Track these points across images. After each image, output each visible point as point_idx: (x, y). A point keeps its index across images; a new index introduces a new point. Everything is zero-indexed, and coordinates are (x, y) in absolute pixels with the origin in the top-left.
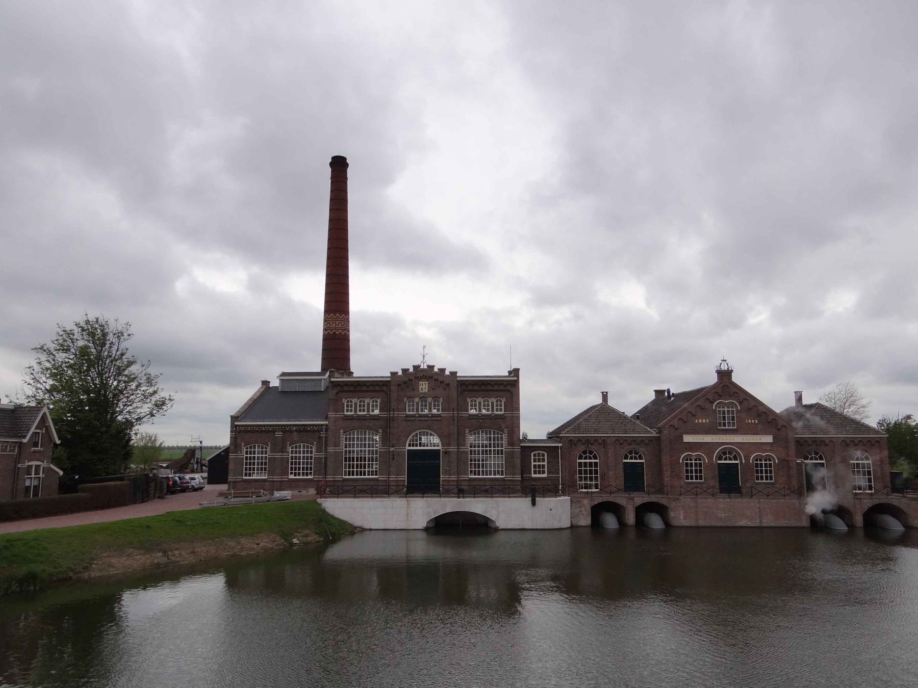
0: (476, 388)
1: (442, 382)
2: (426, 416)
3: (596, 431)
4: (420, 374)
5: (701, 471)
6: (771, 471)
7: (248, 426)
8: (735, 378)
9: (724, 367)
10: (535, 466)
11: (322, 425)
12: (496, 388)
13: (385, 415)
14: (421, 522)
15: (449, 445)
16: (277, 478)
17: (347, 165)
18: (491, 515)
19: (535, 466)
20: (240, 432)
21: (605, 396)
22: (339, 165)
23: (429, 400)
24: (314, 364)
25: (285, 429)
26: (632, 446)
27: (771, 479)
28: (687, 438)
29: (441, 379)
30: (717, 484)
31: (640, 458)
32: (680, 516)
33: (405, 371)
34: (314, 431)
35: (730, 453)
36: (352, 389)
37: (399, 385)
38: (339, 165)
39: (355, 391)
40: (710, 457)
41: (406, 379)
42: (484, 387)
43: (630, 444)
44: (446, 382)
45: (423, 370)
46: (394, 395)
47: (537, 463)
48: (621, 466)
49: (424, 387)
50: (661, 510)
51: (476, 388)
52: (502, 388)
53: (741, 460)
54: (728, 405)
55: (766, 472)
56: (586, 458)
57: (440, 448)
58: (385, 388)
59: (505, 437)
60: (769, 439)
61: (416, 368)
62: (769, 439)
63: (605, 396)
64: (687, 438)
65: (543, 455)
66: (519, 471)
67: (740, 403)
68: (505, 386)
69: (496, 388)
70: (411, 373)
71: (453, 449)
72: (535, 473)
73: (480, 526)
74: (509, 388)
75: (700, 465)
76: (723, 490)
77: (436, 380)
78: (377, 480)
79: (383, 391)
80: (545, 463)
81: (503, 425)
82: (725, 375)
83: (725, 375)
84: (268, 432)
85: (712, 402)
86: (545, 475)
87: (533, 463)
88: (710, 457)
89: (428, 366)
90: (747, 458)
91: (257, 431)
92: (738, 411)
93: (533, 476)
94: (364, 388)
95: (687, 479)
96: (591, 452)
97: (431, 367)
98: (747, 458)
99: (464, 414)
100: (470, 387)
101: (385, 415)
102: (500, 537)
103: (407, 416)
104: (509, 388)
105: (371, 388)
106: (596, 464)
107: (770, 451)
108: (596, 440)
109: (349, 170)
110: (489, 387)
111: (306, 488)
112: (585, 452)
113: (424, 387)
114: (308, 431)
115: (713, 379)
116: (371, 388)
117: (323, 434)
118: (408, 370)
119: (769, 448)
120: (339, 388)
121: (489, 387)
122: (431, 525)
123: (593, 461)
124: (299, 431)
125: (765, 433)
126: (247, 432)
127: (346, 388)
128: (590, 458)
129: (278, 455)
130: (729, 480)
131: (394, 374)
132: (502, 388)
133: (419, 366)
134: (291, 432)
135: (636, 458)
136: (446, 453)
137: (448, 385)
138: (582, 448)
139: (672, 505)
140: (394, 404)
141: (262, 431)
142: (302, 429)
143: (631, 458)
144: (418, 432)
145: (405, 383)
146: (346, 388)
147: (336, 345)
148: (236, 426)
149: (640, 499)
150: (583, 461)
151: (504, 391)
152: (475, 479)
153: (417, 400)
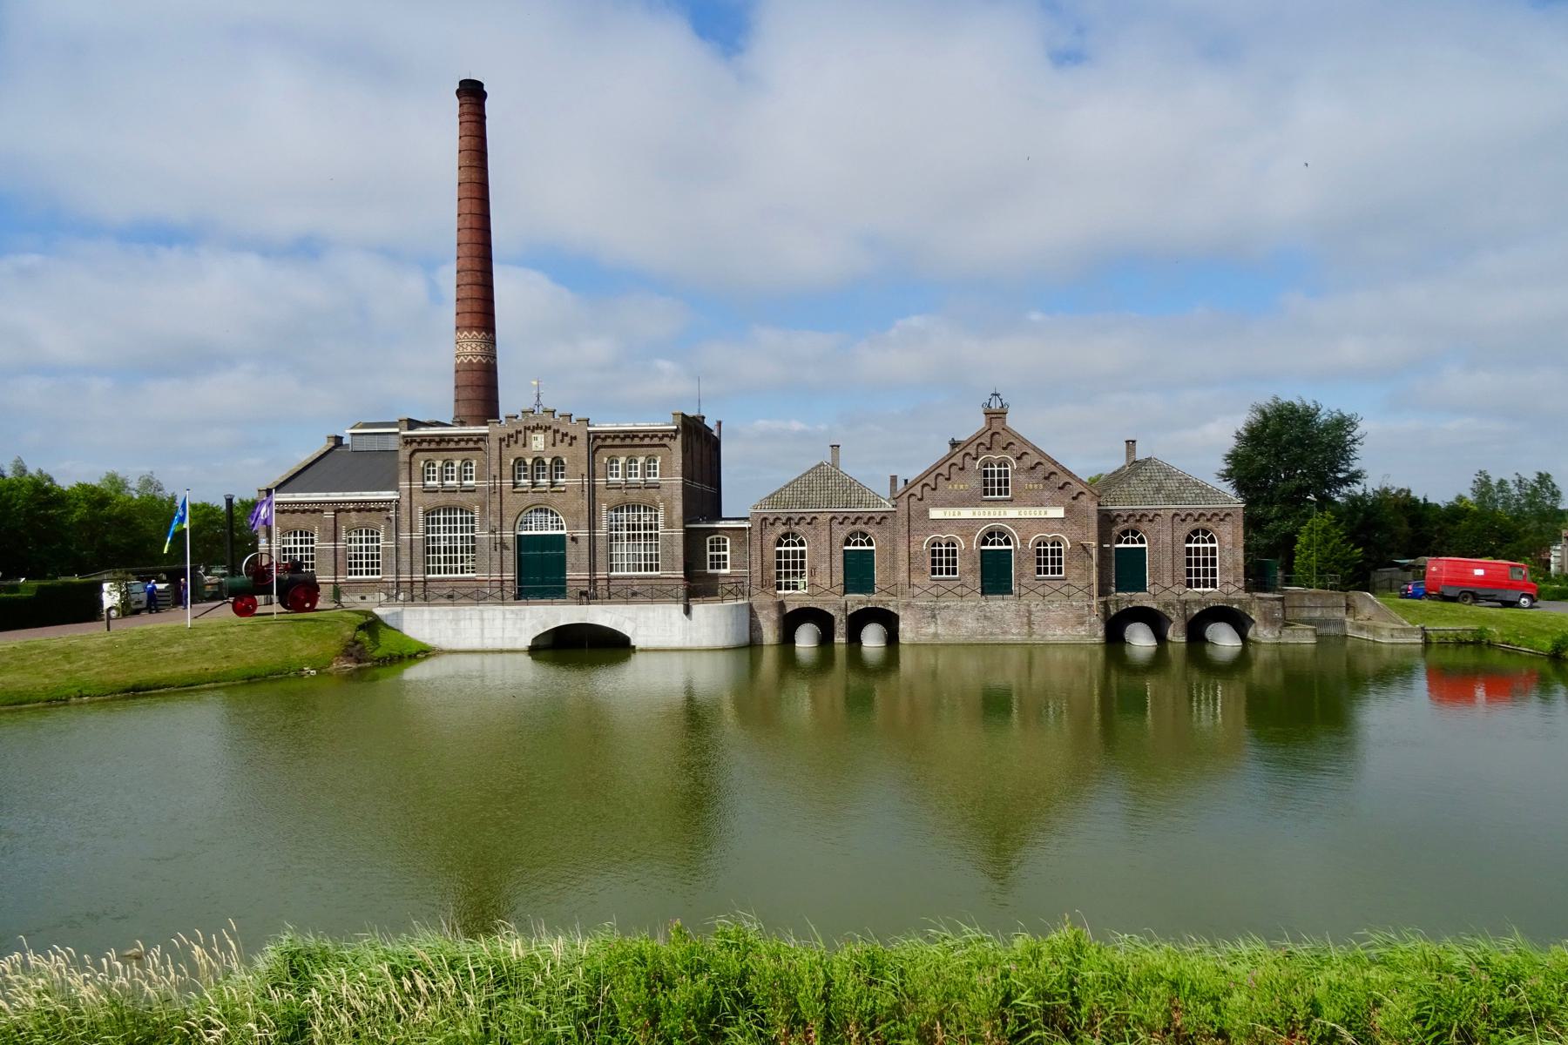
0: (618, 442)
3: (804, 505)
5: (954, 562)
8: (1012, 421)
9: (996, 405)
10: (712, 557)
14: (526, 642)
15: (578, 527)
17: (484, 95)
18: (626, 629)
19: (712, 557)
22: (472, 93)
25: (339, 509)
27: (1060, 572)
28: (935, 513)
30: (978, 583)
34: (380, 510)
36: (433, 446)
37: (501, 440)
38: (472, 93)
42: (628, 442)
49: (538, 442)
50: (889, 621)
56: (787, 545)
60: (1059, 513)
62: (1059, 513)
64: (935, 513)
66: (680, 564)
69: (647, 441)
72: (712, 567)
73: (612, 646)
74: (666, 441)
75: (954, 552)
76: (985, 591)
77: (556, 431)
80: (728, 553)
81: (658, 498)
82: (995, 416)
83: (995, 416)
84: (314, 511)
85: (976, 459)
86: (727, 571)
87: (709, 553)
93: (709, 571)
94: (452, 445)
95: (934, 572)
96: (794, 535)
98: (1024, 541)
100: (609, 442)
102: (637, 660)
104: (666, 441)
105: (462, 445)
106: (802, 554)
107: (1061, 531)
109: (487, 103)
110: (637, 441)
111: (372, 592)
112: (786, 536)
114: (370, 510)
115: (980, 422)
117: (392, 514)
120: (415, 446)
121: (637, 441)
122: (542, 643)
124: (359, 510)
125: (1055, 505)
130: (995, 574)
135: (862, 544)
139: (901, 614)
142: (363, 507)
145: (510, 436)
149: (857, 601)
152: (616, 578)
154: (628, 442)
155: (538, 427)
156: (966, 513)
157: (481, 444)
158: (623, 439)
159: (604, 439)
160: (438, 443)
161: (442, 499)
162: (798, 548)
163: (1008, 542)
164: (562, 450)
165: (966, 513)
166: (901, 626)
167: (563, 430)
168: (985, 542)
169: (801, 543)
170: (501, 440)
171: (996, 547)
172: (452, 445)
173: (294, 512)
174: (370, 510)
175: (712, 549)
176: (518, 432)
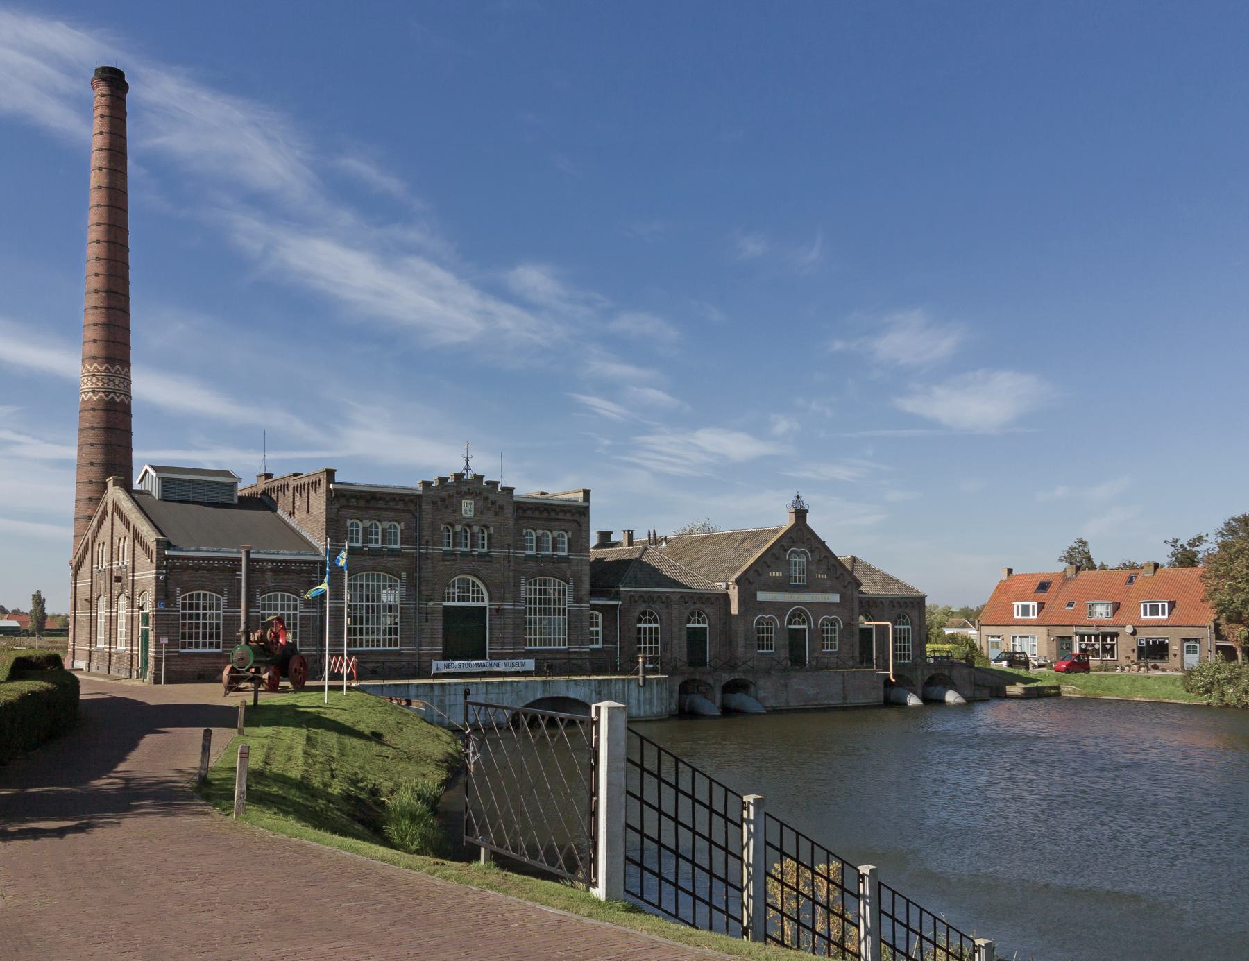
1: (493, 503)
2: (470, 554)
4: (464, 488)
7: (189, 558)
12: (561, 516)
13: (408, 549)
15: (503, 599)
20: (174, 567)
23: (476, 529)
28: (762, 596)
29: (492, 497)
33: (442, 480)
35: (800, 616)
39: (367, 508)
40: (782, 622)
41: (444, 494)
42: (545, 515)
44: (500, 502)
45: (467, 481)
46: (427, 519)
48: (685, 632)
49: (468, 507)
51: (536, 514)
52: (568, 516)
54: (798, 554)
56: (645, 622)
57: (486, 603)
58: (411, 507)
59: (569, 589)
60: (835, 598)
61: (458, 476)
62: (835, 598)
64: (762, 596)
65: (597, 617)
67: (812, 552)
70: (449, 486)
71: (508, 605)
77: (486, 499)
78: (398, 653)
80: (599, 629)
81: (569, 572)
86: (599, 646)
88: (782, 622)
90: (816, 624)
91: (204, 568)
96: (651, 614)
97: (479, 478)
98: (816, 624)
99: (521, 553)
101: (408, 549)
103: (445, 553)
104: (577, 517)
106: (656, 628)
108: (659, 595)
112: (644, 613)
113: (468, 507)
116: (392, 504)
118: (446, 479)
120: (343, 500)
123: (653, 625)
125: (834, 591)
126: (185, 568)
131: (426, 484)
133: (462, 475)
134: (263, 571)
136: (497, 611)
137: (501, 507)
138: (642, 607)
140: (427, 534)
141: (214, 569)
145: (443, 500)
148: (167, 558)
151: (570, 521)
153: (458, 528)
159: (524, 511)
160: (368, 501)
162: (653, 625)
163: (804, 623)
164: (489, 517)
168: (790, 622)
169: (655, 621)
171: (797, 627)
172: (381, 504)
173: (199, 569)
174: (287, 571)
176: (450, 496)
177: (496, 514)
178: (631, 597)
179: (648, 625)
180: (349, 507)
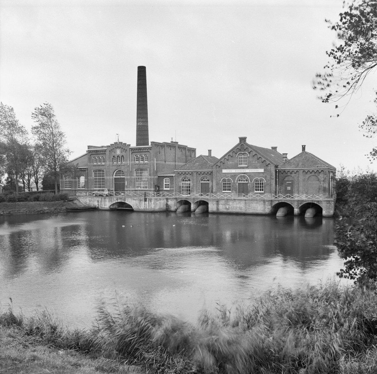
0: (137, 151)
6: (256, 187)
8: (248, 141)
11: (86, 168)
16: (73, 189)
19: (165, 184)
21: (210, 151)
24: (131, 140)
26: (204, 175)
28: (224, 171)
31: (208, 181)
32: (212, 207)
34: (84, 171)
40: (234, 180)
42: (139, 151)
43: (203, 174)
47: (166, 183)
51: (137, 151)
53: (249, 181)
54: (243, 154)
55: (260, 187)
56: (185, 181)
60: (262, 170)
62: (262, 170)
63: (210, 151)
64: (224, 171)
67: (249, 153)
68: (148, 150)
69: (144, 150)
72: (165, 187)
77: (122, 148)
79: (105, 154)
82: (243, 140)
83: (243, 140)
85: (236, 153)
87: (164, 183)
88: (234, 180)
89: (120, 143)
92: (248, 157)
93: (165, 189)
94: (99, 153)
97: (122, 143)
104: (149, 150)
110: (142, 151)
119: (262, 175)
120: (91, 153)
121: (142, 151)
123: (188, 182)
125: (261, 168)
127: (93, 153)
128: (187, 181)
129: (74, 180)
132: (146, 150)
133: (117, 143)
135: (206, 181)
137: (126, 150)
143: (204, 181)
144: (118, 170)
145: (112, 150)
146: (93, 153)
147: (142, 132)
150: (184, 182)
154: (139, 151)
155: (118, 147)
156: (233, 171)
157: (105, 153)
158: (138, 150)
161: (97, 168)
163: (247, 181)
165: (233, 171)
166: (209, 205)
167: (124, 148)
169: (189, 180)
170: (110, 151)
171: (243, 182)
175: (165, 182)
176: (113, 149)
177: (125, 152)
178: (179, 173)
179: (186, 182)
180: (92, 154)
